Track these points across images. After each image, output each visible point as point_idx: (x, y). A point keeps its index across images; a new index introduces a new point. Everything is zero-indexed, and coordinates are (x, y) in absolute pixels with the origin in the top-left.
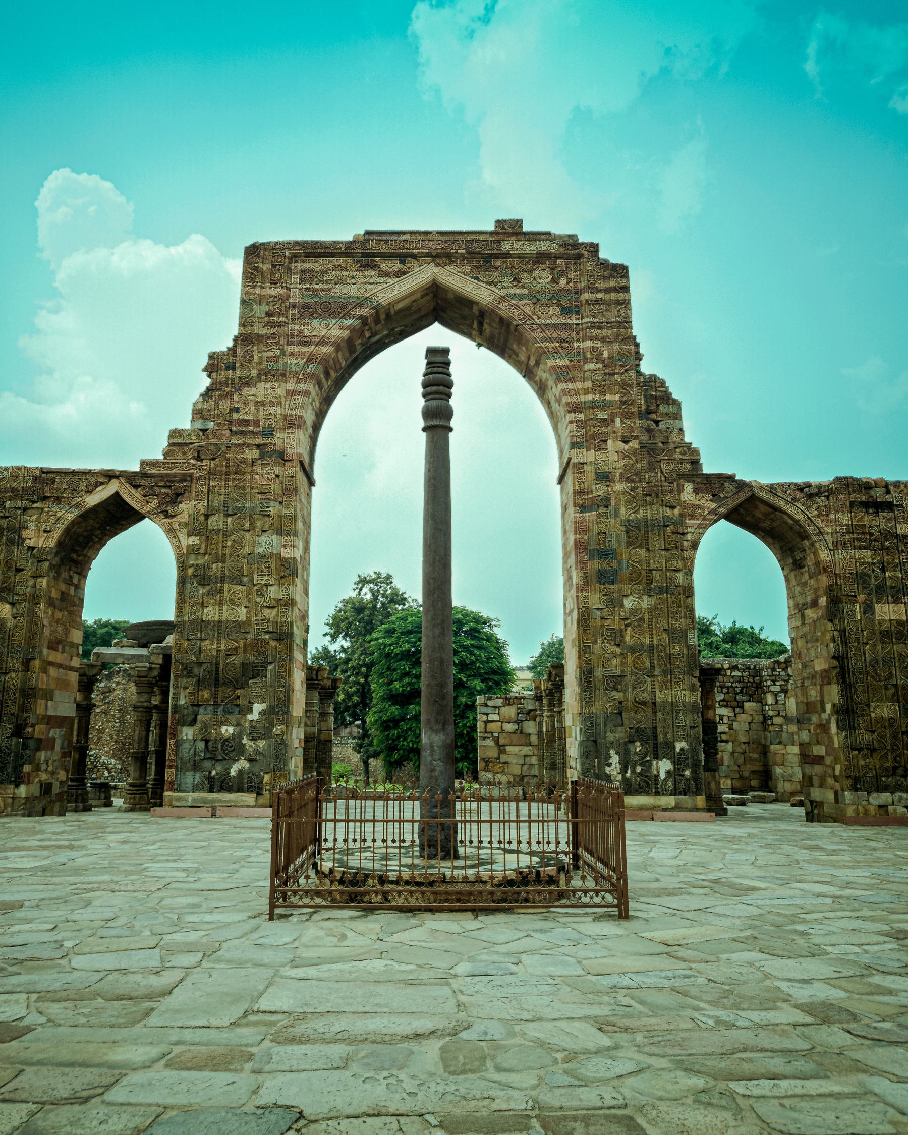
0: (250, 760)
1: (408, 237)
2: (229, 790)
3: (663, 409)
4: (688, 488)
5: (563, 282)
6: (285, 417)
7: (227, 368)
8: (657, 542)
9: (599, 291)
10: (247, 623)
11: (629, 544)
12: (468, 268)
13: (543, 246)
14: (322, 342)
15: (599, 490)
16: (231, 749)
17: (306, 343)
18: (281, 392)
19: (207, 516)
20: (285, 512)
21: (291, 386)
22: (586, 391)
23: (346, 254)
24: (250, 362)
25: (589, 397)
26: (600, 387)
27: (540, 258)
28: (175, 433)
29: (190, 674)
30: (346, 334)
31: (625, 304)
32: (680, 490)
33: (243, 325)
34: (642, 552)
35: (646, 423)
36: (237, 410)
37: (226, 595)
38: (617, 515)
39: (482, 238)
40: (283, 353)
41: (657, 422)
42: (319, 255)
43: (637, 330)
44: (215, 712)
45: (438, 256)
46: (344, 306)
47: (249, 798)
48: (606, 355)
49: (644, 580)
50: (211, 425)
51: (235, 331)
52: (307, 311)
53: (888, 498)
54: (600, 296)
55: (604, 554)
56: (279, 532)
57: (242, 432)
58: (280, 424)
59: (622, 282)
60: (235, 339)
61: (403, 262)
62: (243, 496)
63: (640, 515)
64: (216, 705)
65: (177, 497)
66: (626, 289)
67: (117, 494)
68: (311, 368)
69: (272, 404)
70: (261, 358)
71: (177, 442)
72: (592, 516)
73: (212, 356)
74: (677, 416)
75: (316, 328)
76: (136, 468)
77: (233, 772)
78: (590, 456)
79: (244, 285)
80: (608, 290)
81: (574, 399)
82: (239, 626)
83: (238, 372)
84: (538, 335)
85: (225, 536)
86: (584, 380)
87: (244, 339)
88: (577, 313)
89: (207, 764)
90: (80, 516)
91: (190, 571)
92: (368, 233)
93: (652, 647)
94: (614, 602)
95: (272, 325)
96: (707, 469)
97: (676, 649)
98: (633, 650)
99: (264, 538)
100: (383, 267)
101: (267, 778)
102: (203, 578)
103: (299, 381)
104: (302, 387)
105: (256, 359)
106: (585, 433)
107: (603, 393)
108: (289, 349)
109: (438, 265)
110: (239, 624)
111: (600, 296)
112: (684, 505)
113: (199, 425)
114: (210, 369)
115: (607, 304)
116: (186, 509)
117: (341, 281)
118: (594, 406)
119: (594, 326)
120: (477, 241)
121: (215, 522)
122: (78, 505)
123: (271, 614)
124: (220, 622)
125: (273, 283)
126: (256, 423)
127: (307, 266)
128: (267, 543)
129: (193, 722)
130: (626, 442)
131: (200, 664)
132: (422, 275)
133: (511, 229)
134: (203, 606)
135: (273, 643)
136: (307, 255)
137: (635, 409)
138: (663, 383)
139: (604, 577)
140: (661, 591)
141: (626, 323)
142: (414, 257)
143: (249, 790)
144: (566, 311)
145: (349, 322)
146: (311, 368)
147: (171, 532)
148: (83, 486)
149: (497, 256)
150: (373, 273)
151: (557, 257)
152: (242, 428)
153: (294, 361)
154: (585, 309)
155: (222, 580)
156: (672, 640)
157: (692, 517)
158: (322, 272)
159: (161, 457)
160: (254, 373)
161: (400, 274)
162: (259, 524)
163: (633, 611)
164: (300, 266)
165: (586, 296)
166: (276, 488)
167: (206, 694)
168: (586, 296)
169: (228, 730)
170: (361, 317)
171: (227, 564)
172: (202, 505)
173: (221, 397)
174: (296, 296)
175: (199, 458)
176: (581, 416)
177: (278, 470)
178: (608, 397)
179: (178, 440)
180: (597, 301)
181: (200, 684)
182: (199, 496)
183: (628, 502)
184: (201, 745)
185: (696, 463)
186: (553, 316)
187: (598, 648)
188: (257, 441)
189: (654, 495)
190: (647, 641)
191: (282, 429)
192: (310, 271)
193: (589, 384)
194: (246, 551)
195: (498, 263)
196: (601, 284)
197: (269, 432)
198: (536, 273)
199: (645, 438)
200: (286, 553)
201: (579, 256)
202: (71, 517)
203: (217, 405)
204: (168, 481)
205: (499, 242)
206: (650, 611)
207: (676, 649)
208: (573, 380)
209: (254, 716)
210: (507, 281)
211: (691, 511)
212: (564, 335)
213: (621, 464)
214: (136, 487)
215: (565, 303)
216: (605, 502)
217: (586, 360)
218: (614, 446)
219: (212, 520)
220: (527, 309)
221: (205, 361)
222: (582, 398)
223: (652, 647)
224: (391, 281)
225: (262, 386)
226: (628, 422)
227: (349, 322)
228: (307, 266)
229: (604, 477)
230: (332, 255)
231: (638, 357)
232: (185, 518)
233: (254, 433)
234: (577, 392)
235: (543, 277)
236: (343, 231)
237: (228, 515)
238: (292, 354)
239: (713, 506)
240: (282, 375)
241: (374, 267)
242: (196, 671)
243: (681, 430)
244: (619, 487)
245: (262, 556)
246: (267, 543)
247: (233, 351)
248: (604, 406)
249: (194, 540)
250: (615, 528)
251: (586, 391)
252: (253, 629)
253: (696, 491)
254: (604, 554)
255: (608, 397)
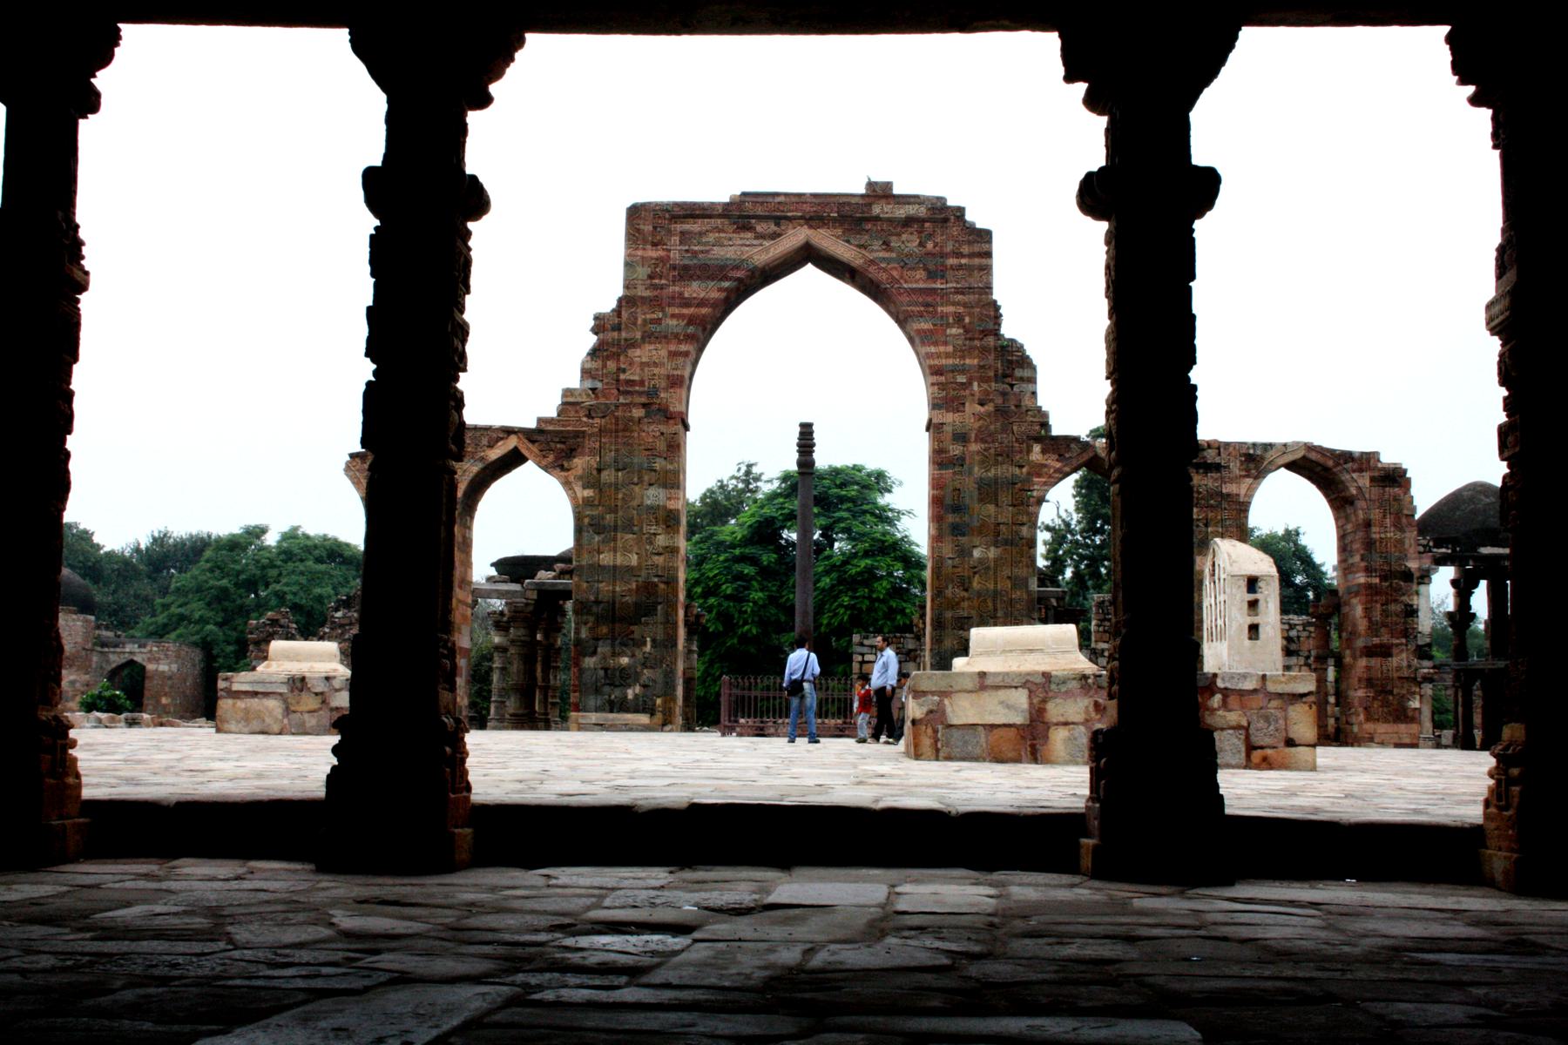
0: (644, 686)
1: (781, 199)
2: (627, 711)
3: (1018, 373)
4: (1037, 448)
5: (930, 245)
6: (668, 377)
7: (613, 329)
8: (1005, 499)
9: (962, 256)
10: (639, 567)
11: (981, 500)
12: (839, 232)
13: (911, 210)
14: (702, 303)
15: (955, 450)
16: (623, 677)
17: (686, 303)
18: (664, 353)
19: (599, 471)
20: (670, 467)
21: (673, 348)
22: (947, 355)
23: (719, 216)
24: (635, 324)
25: (950, 361)
26: (961, 352)
27: (908, 222)
28: (567, 392)
29: (589, 613)
30: (723, 295)
31: (987, 269)
32: (1029, 451)
33: (626, 287)
34: (991, 508)
35: (1001, 387)
36: (624, 371)
37: (619, 544)
38: (970, 473)
39: (853, 201)
40: (665, 315)
41: (1012, 386)
42: (698, 217)
43: (997, 295)
44: (613, 646)
45: (811, 218)
46: (722, 268)
47: (644, 719)
48: (967, 320)
49: (994, 534)
50: (599, 385)
51: (620, 292)
52: (685, 273)
53: (1217, 460)
54: (963, 261)
55: (957, 509)
56: (665, 486)
57: (627, 393)
58: (663, 384)
59: (985, 247)
60: (620, 300)
61: (777, 224)
62: (631, 453)
63: (991, 474)
64: (614, 639)
65: (571, 453)
66: (989, 255)
67: (516, 448)
68: (691, 330)
69: (655, 364)
70: (645, 320)
71: (569, 402)
72: (948, 473)
73: (597, 318)
74: (1032, 380)
75: (695, 289)
76: (532, 425)
77: (630, 694)
78: (949, 417)
79: (628, 247)
80: (971, 255)
81: (936, 362)
82: (629, 570)
83: (624, 335)
84: (905, 299)
85: (617, 489)
86: (946, 343)
87: (625, 302)
88: (943, 277)
89: (607, 689)
90: (483, 469)
91: (586, 521)
92: (744, 194)
93: (995, 592)
94: (964, 553)
95: (655, 287)
96: (1055, 432)
97: (1017, 595)
98: (979, 594)
99: (652, 491)
100: (759, 228)
101: (659, 701)
102: (598, 527)
103: (680, 342)
104: (683, 348)
105: (639, 321)
106: (946, 394)
107: (963, 357)
108: (671, 310)
109: (811, 227)
110: (629, 569)
111: (963, 261)
112: (1029, 463)
113: (589, 384)
114: (596, 330)
115: (970, 269)
116: (580, 463)
117: (718, 243)
118: (955, 370)
119: (958, 291)
120: (849, 204)
121: (607, 476)
122: (482, 459)
123: (659, 560)
124: (615, 567)
125: (655, 245)
126: (642, 383)
127: (686, 227)
128: (654, 496)
129: (594, 653)
130: (982, 405)
131: (597, 602)
132: (796, 237)
133: (880, 192)
134: (599, 553)
135: (662, 586)
136: (686, 217)
137: (992, 374)
138: (1020, 348)
139: (957, 530)
140: (1006, 542)
141: (988, 288)
142: (786, 218)
143: (644, 711)
144: (932, 276)
145: (726, 284)
146: (691, 330)
147: (567, 484)
148: (485, 441)
149: (868, 220)
150: (749, 235)
151: (924, 221)
152: (625, 388)
153: (674, 322)
154: (950, 274)
155: (615, 528)
156: (1014, 586)
157: (1039, 475)
158: (701, 234)
159: (554, 415)
160: (638, 335)
161: (775, 236)
162: (646, 478)
163: (981, 561)
164: (679, 227)
165: (951, 261)
166: (661, 445)
167: (604, 630)
168: (951, 261)
169: (625, 660)
170: (738, 279)
171: (620, 513)
172: (594, 461)
173: (608, 358)
174: (675, 256)
175: (589, 416)
176: (942, 379)
177: (663, 428)
178: (968, 361)
179: (571, 400)
180: (960, 267)
181: (600, 620)
182: (592, 452)
183: (982, 462)
184: (602, 673)
185: (1045, 425)
186: (918, 279)
187: (949, 592)
188: (643, 400)
189: (1006, 455)
190: (992, 587)
191: (666, 389)
192: (689, 233)
193: (950, 349)
194: (635, 503)
195: (869, 226)
196: (965, 249)
197: (653, 393)
198: (904, 237)
199: (999, 401)
200: (671, 505)
201: (946, 220)
202: (475, 469)
203: (605, 366)
204: (563, 437)
205: (870, 205)
206: (996, 560)
207: (1017, 595)
208: (936, 344)
209: (648, 648)
210: (877, 245)
211: (1038, 470)
212: (929, 299)
213: (977, 425)
214: (533, 442)
215: (931, 267)
216: (960, 461)
217: (949, 325)
218: (972, 408)
219: (604, 474)
220: (895, 273)
221: (592, 323)
222: (944, 362)
223: (995, 592)
224: (766, 243)
225: (648, 347)
226: (985, 386)
227: (726, 284)
228: (686, 227)
229: (961, 438)
230: (710, 217)
231: (997, 318)
232: (580, 472)
233: (640, 394)
234: (939, 356)
235: (909, 242)
236: (718, 192)
237: (618, 470)
238: (673, 316)
239: (1058, 465)
240: (663, 338)
241: (750, 228)
242: (595, 609)
243: (1034, 393)
244: (974, 447)
245: (650, 508)
246: (654, 496)
247: (618, 311)
248: (963, 371)
249: (588, 493)
250: (969, 485)
251: (947, 355)
252: (644, 573)
253: (1043, 452)
254: (957, 509)
255: (968, 361)
